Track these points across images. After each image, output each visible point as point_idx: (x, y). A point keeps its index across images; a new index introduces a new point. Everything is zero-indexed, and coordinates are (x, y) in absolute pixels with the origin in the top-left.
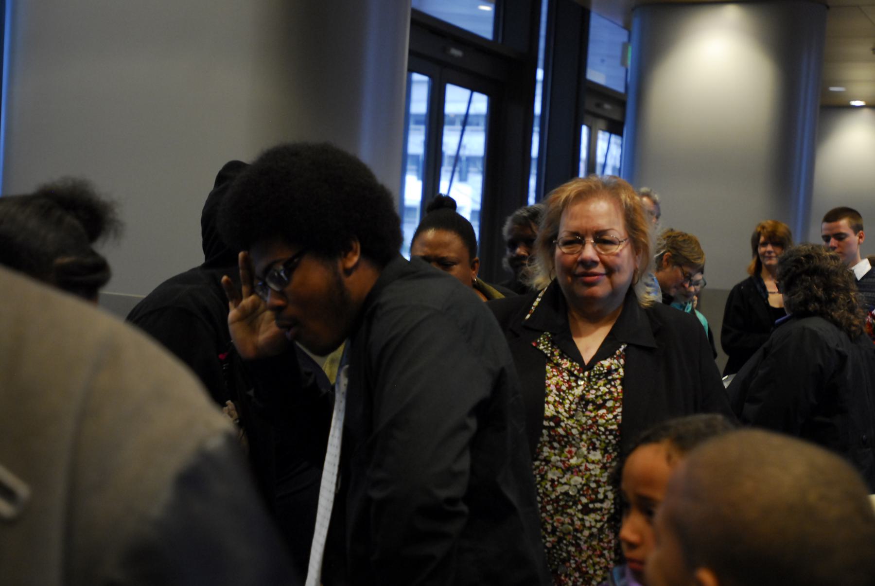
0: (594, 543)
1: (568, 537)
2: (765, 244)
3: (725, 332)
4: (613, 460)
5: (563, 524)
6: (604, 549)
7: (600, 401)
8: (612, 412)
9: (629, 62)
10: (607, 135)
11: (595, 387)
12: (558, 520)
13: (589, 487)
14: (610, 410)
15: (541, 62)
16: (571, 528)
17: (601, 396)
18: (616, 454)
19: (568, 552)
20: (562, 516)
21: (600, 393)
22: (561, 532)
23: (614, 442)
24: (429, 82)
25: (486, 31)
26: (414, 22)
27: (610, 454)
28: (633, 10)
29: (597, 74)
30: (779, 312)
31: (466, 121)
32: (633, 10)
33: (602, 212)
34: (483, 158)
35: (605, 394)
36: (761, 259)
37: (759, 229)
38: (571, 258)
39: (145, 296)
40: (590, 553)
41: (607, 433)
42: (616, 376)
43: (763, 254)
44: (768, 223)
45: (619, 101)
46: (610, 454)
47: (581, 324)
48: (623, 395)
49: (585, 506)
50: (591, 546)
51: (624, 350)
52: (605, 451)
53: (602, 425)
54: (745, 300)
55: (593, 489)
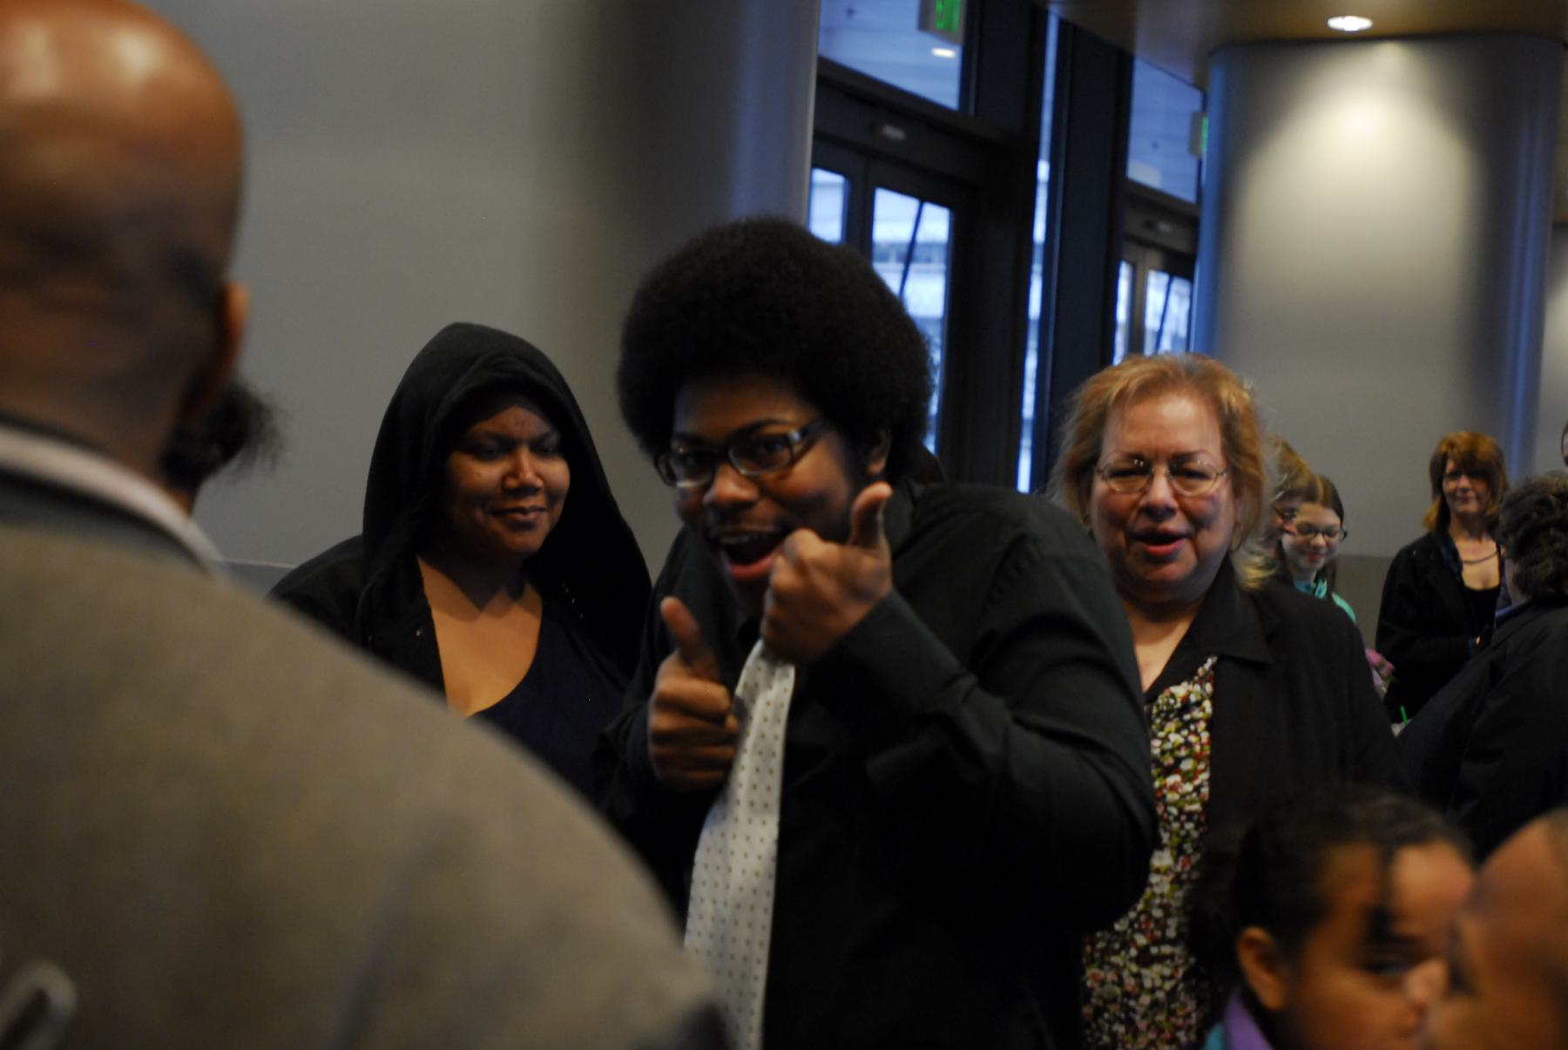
0: (1161, 1018)
1: (1113, 1008)
2: (1455, 475)
3: (1383, 633)
4: (1193, 868)
5: (1103, 983)
6: (1178, 1028)
7: (1169, 760)
8: (1191, 780)
9: (1204, 148)
10: (1164, 278)
11: (1161, 734)
12: (1094, 976)
13: (1150, 917)
14: (1188, 777)
15: (1045, 149)
16: (1118, 991)
17: (1172, 751)
18: (1198, 856)
19: (1113, 1035)
20: (1101, 967)
21: (1168, 746)
22: (1100, 997)
23: (1195, 834)
24: (845, 186)
25: (945, 92)
26: (821, 81)
27: (1189, 856)
28: (1211, 54)
29: (1144, 170)
30: (1488, 597)
31: (909, 254)
32: (1211, 54)
33: (1181, 418)
34: (942, 321)
35: (1179, 747)
36: (1449, 501)
37: (1444, 448)
38: (1125, 500)
39: (294, 566)
40: (1152, 1035)
41: (1183, 818)
42: (1197, 714)
43: (1453, 494)
44: (1461, 437)
45: (1185, 217)
46: (1189, 856)
47: (1135, 621)
48: (1212, 749)
49: (1144, 951)
50: (1153, 1022)
51: (1213, 667)
52: (1179, 851)
53: (1175, 804)
54: (1422, 574)
55: (1157, 921)
